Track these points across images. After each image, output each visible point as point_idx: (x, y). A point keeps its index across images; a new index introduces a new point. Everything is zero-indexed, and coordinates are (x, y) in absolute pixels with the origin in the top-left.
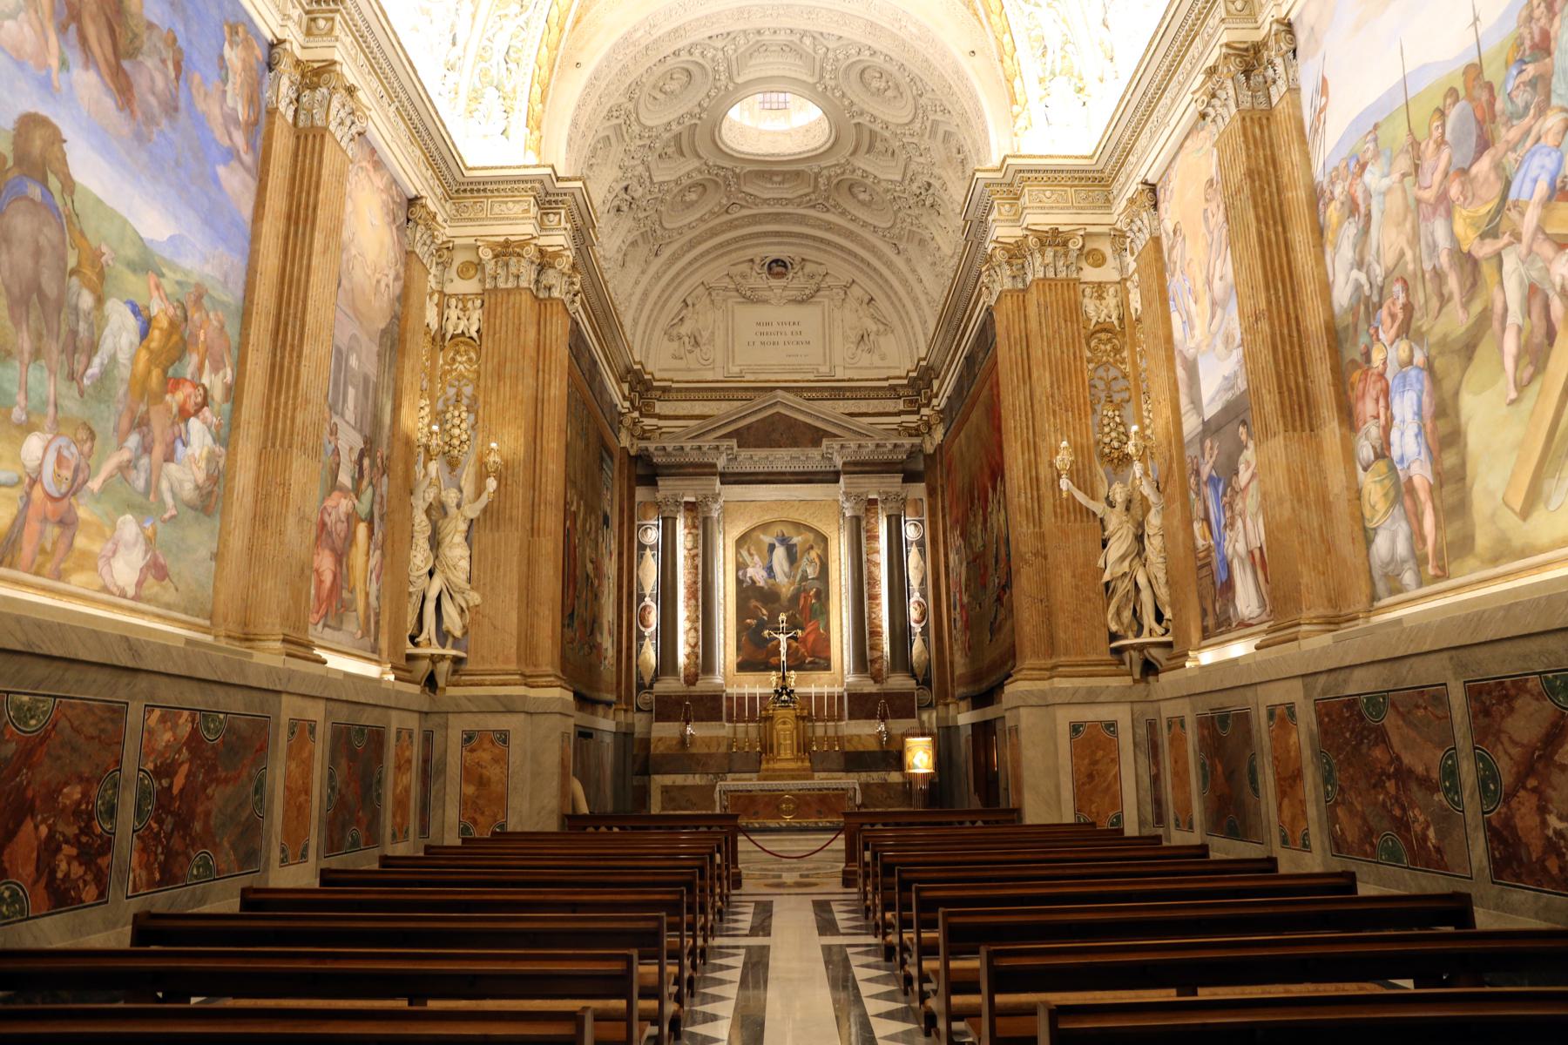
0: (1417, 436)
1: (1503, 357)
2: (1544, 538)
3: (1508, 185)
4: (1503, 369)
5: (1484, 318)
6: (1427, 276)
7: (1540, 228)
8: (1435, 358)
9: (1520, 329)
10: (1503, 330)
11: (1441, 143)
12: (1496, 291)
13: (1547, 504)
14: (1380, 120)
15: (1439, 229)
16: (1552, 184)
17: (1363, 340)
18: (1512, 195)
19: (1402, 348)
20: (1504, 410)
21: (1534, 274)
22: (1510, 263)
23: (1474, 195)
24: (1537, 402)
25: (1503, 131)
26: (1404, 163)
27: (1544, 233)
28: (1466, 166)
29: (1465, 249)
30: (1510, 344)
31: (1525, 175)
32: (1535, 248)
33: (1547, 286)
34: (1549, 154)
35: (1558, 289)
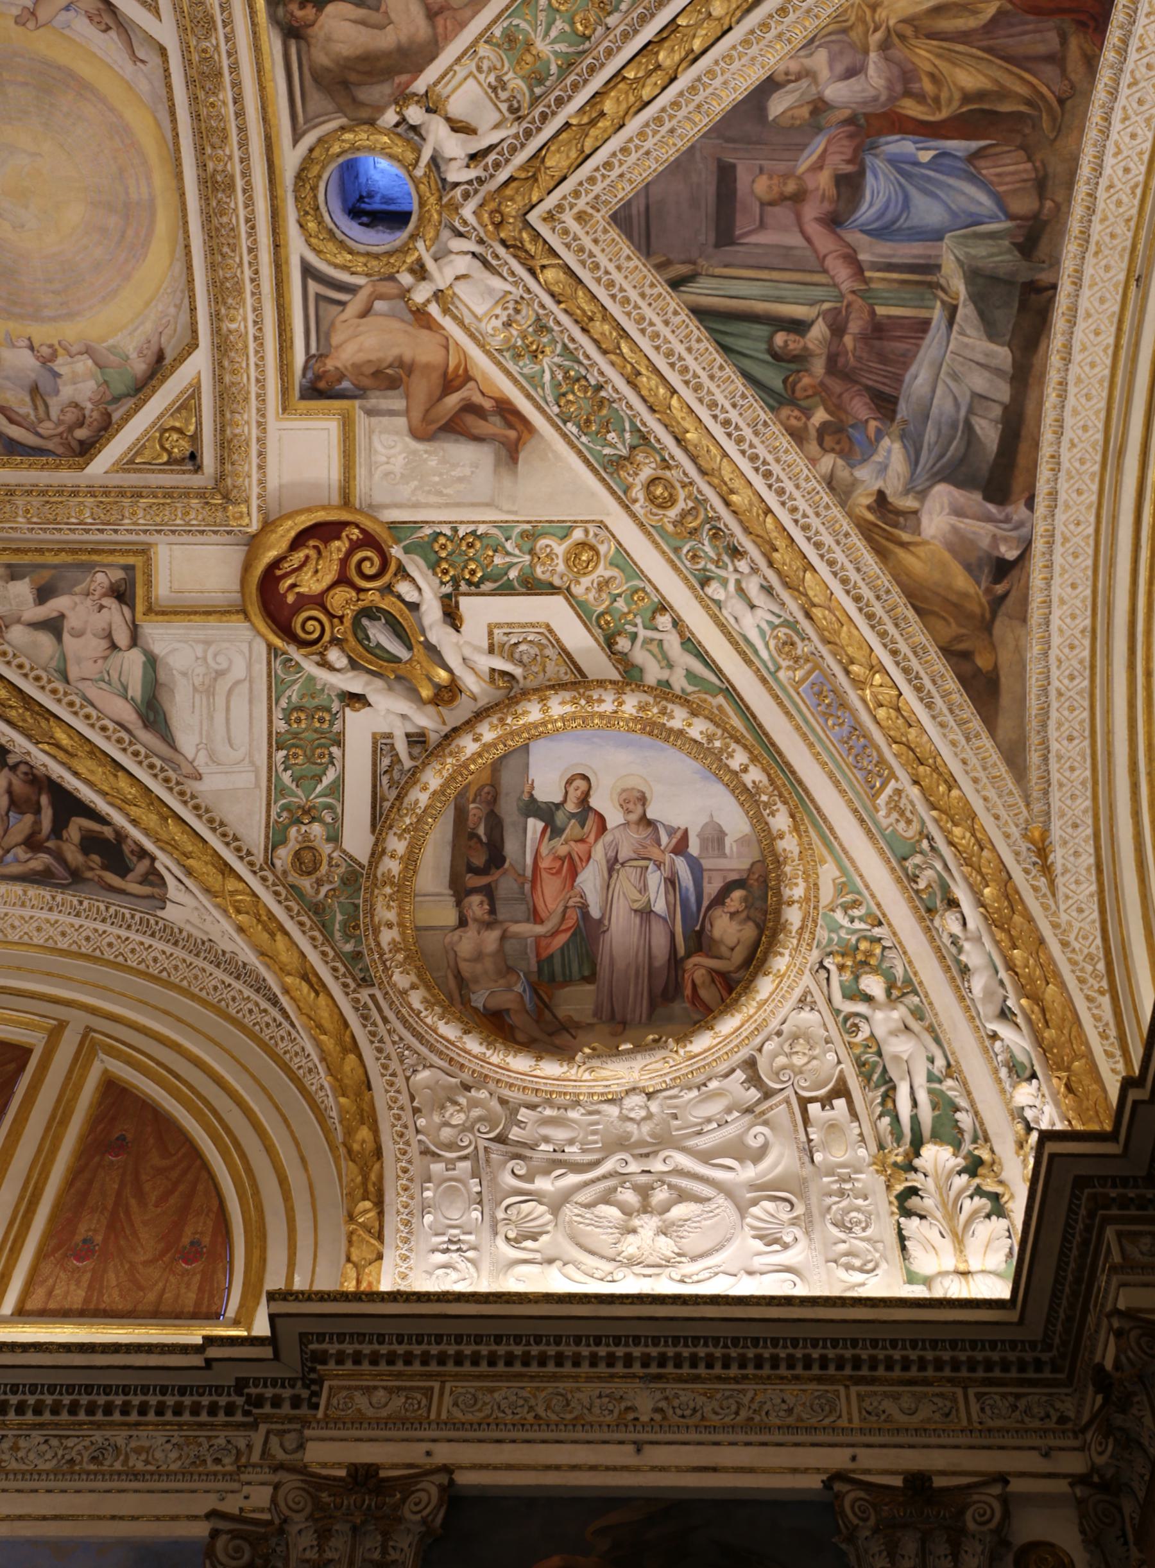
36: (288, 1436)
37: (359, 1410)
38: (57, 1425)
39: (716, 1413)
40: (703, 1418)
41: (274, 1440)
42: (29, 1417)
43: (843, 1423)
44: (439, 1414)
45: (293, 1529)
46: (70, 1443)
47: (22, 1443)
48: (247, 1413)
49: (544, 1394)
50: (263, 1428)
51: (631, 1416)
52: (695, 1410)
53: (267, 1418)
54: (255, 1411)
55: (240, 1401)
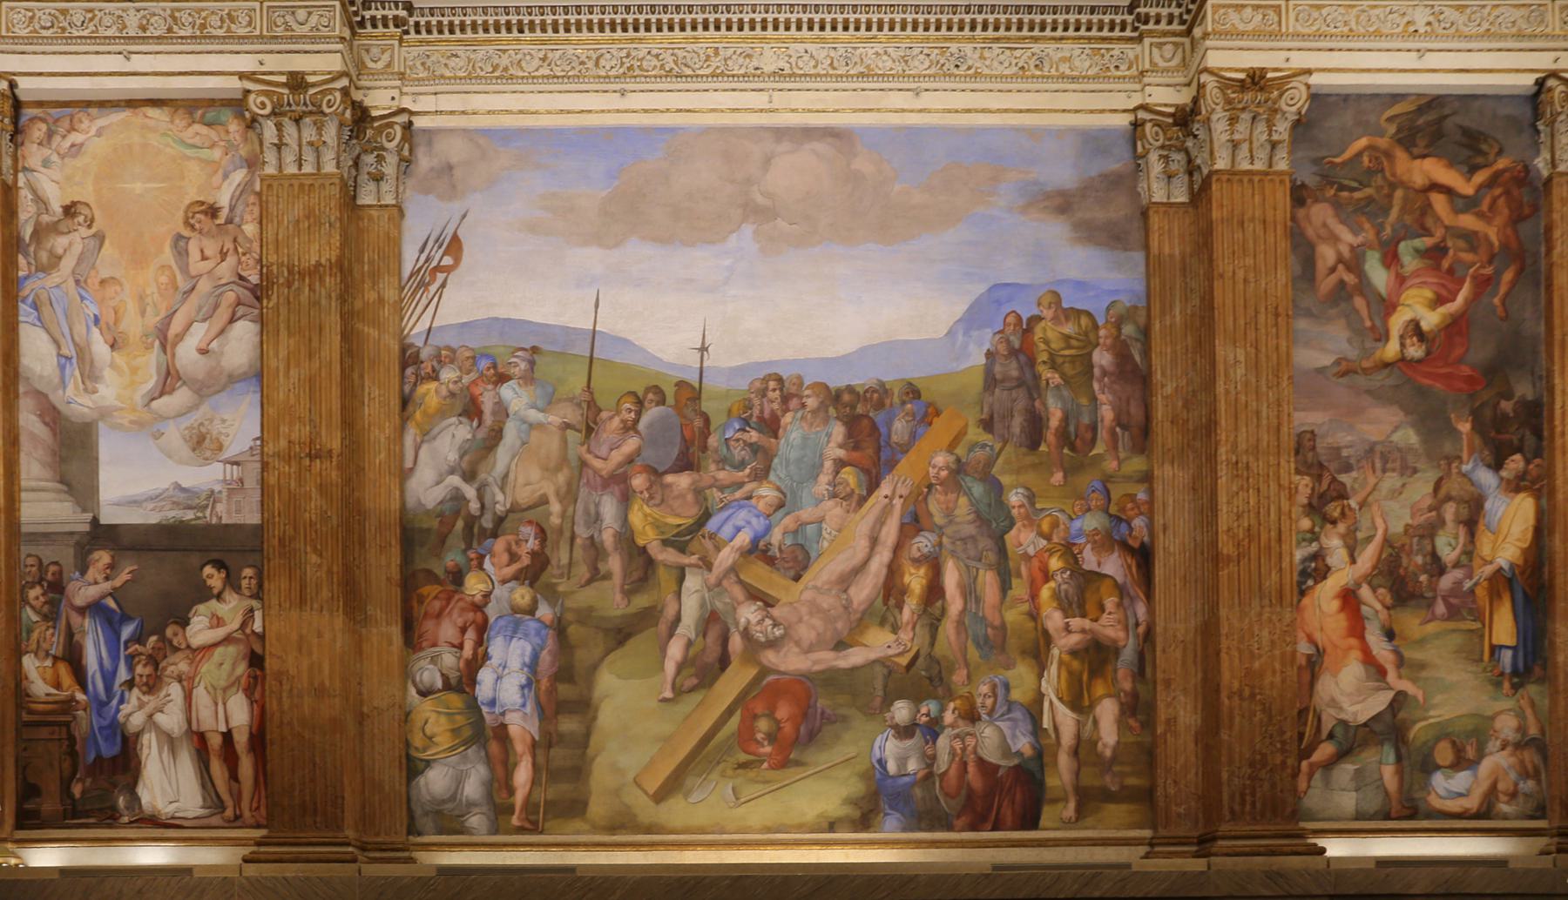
0: (522, 687)
1: (664, 657)
2: (678, 822)
3: (706, 516)
4: (662, 669)
5: (648, 617)
6: (578, 541)
7: (733, 570)
8: (570, 623)
9: (690, 644)
10: (671, 635)
11: (630, 427)
12: (670, 598)
13: (686, 796)
14: (545, 347)
15: (609, 508)
16: (755, 542)
17: (452, 558)
18: (712, 525)
19: (522, 595)
20: (654, 704)
21: (719, 605)
22: (692, 582)
23: (663, 501)
24: (694, 711)
25: (713, 467)
26: (572, 415)
27: (738, 576)
28: (661, 469)
29: (641, 542)
30: (675, 650)
31: (728, 518)
32: (725, 583)
33: (730, 621)
34: (758, 516)
35: (741, 629)
36: (1165, 47)
37: (1233, 25)
38: (1008, 39)
39: (1466, 25)
40: (1457, 30)
41: (1155, 50)
42: (990, 33)
43: (1549, 30)
44: (1287, 28)
45: (1214, 117)
46: (1018, 53)
47: (987, 54)
48: (1135, 29)
49: (1355, 10)
50: (1147, 41)
51: (1412, 29)
52: (1452, 24)
53: (1151, 33)
54: (1143, 27)
55: (1129, 18)
